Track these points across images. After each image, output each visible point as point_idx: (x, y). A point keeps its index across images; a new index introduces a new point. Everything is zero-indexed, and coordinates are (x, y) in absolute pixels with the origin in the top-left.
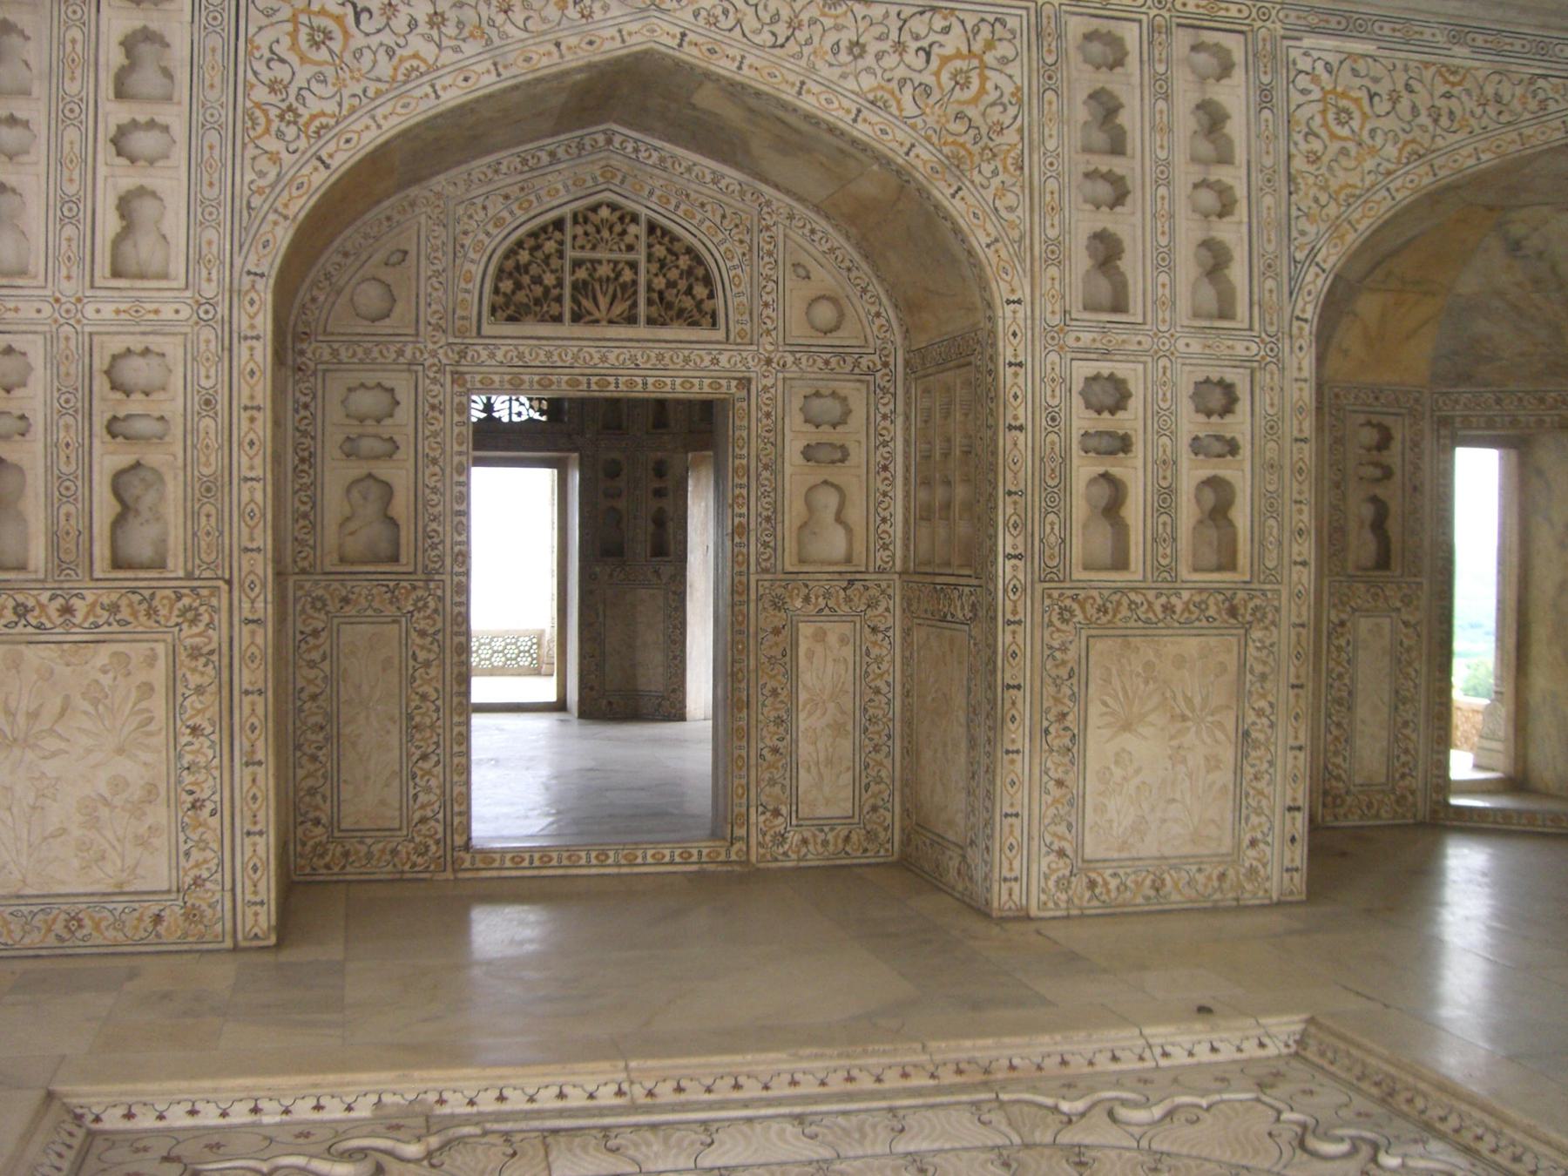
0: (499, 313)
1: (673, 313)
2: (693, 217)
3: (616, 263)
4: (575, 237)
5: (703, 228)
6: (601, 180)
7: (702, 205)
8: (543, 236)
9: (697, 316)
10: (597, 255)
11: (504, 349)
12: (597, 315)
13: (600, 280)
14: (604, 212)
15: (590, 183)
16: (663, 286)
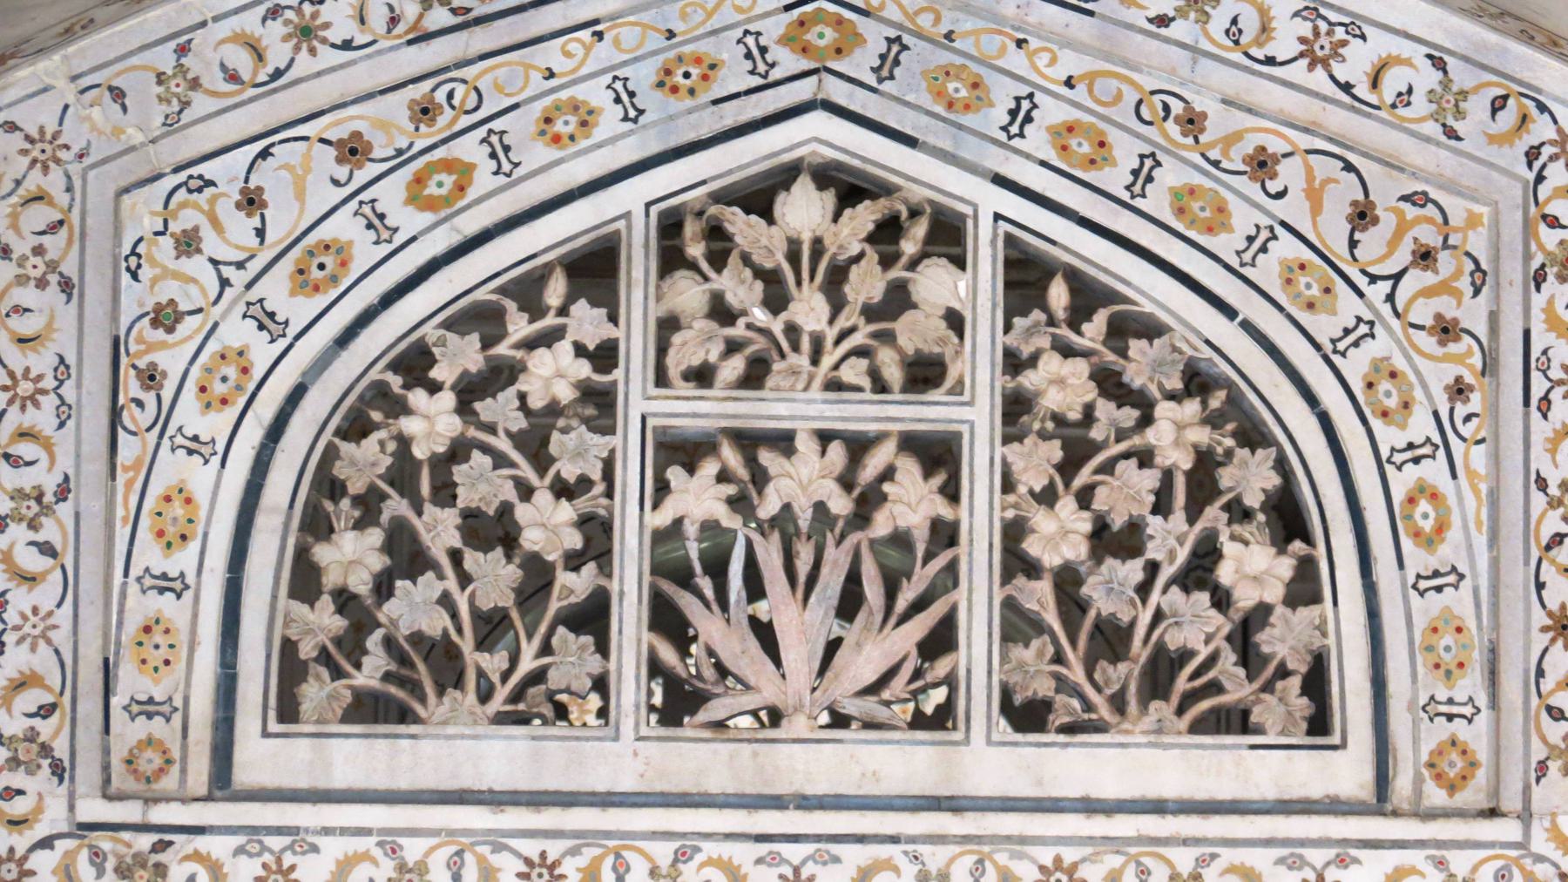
0: (316, 692)
1: (1125, 673)
2: (1219, 220)
3: (859, 446)
4: (669, 325)
5: (1267, 272)
6: (789, 61)
7: (1262, 164)
8: (519, 326)
9: (1237, 688)
10: (766, 409)
11: (333, 848)
12: (769, 690)
13: (784, 521)
14: (804, 210)
15: (735, 77)
16: (1076, 550)
